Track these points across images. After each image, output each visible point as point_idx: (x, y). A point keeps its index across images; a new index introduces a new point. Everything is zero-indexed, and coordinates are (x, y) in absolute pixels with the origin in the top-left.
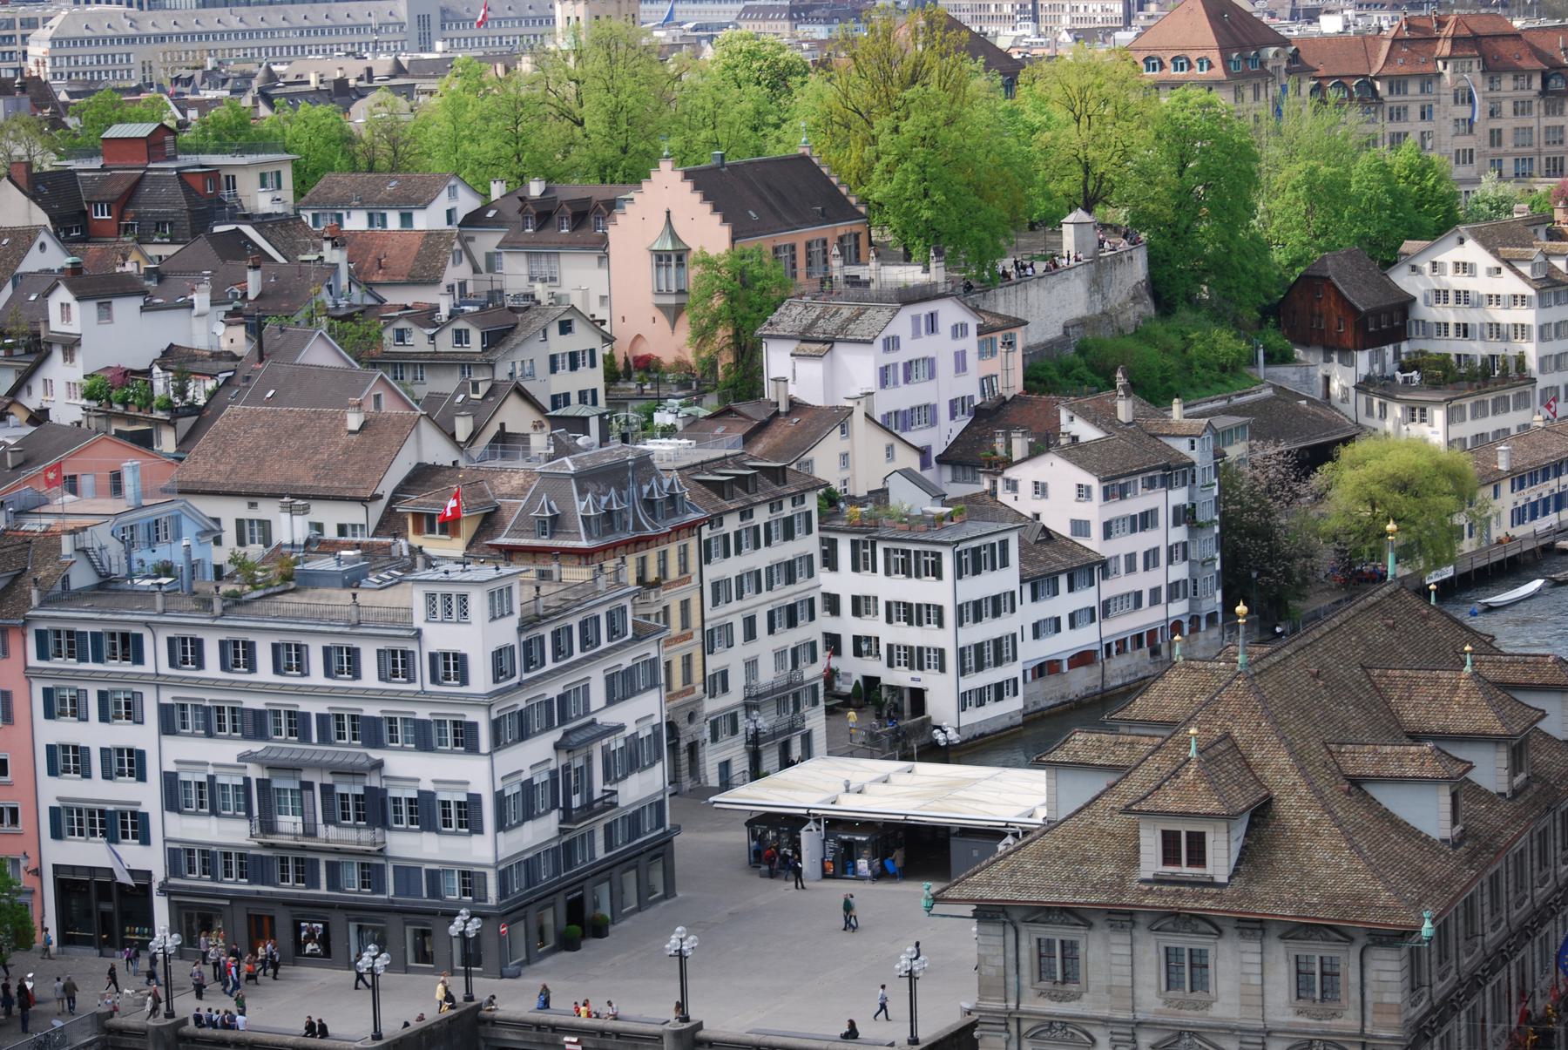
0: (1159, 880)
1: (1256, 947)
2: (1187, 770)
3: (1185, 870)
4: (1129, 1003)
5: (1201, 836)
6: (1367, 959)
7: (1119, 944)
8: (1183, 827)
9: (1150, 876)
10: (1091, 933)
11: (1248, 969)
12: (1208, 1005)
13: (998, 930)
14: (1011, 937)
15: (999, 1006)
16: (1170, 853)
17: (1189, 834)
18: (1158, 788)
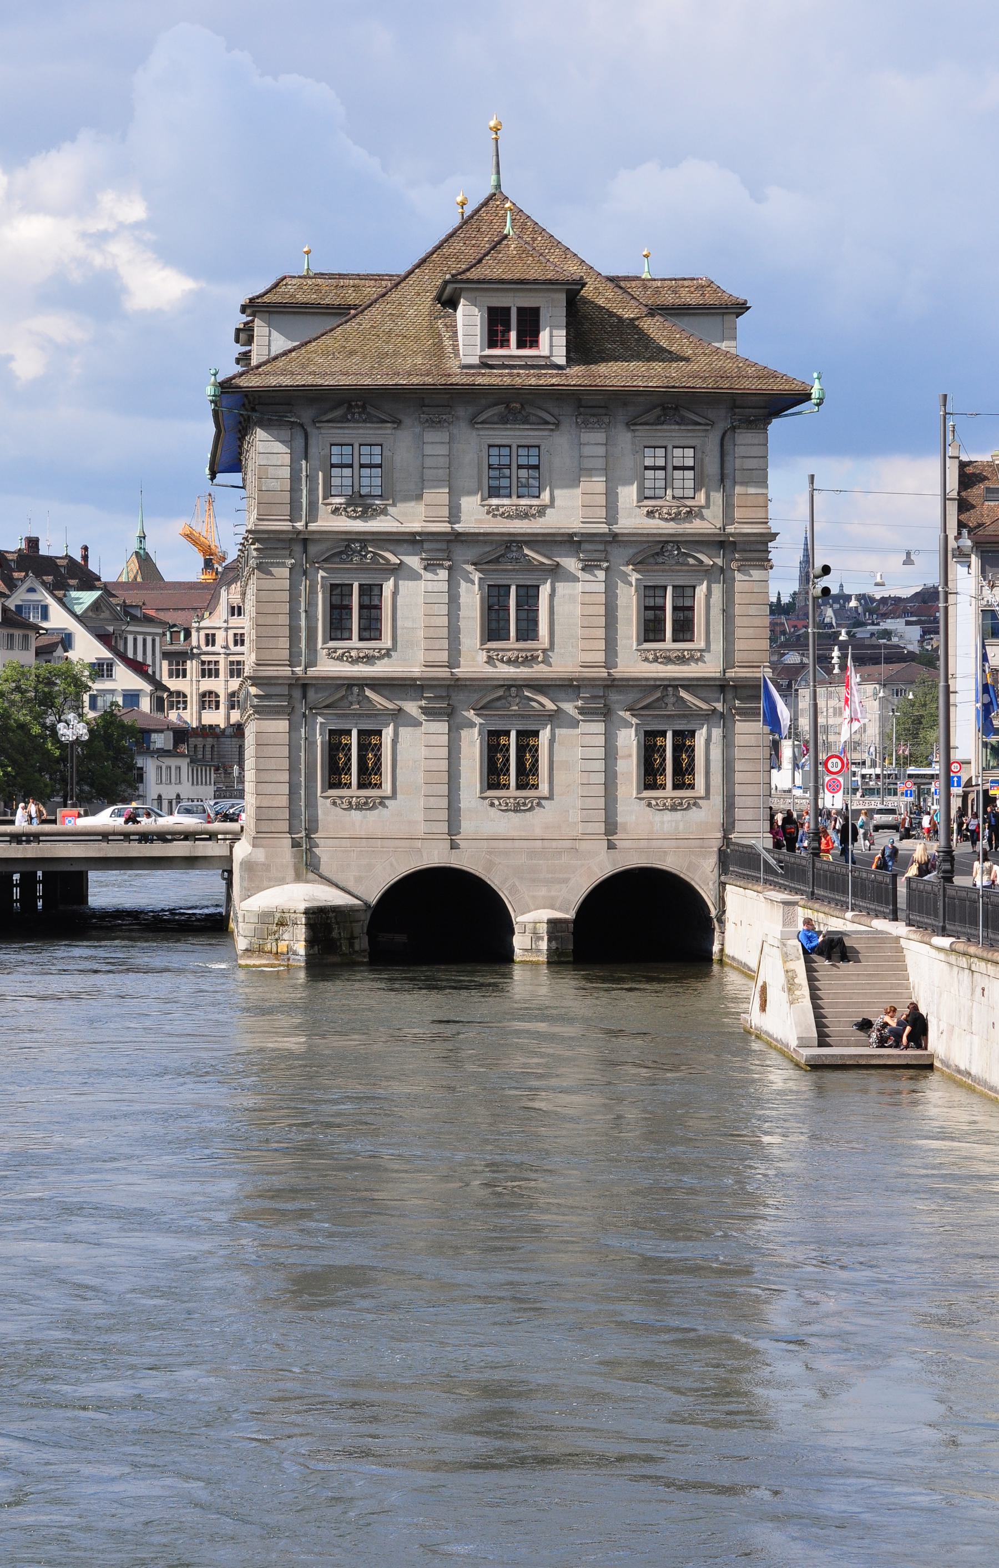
0: (485, 364)
1: (600, 437)
2: (508, 246)
3: (513, 350)
4: (445, 512)
5: (535, 312)
6: (728, 447)
7: (435, 444)
8: (514, 302)
9: (476, 361)
10: (399, 432)
11: (588, 464)
12: (542, 511)
13: (286, 434)
14: (300, 442)
15: (285, 526)
16: (495, 337)
17: (520, 310)
18: (480, 261)
